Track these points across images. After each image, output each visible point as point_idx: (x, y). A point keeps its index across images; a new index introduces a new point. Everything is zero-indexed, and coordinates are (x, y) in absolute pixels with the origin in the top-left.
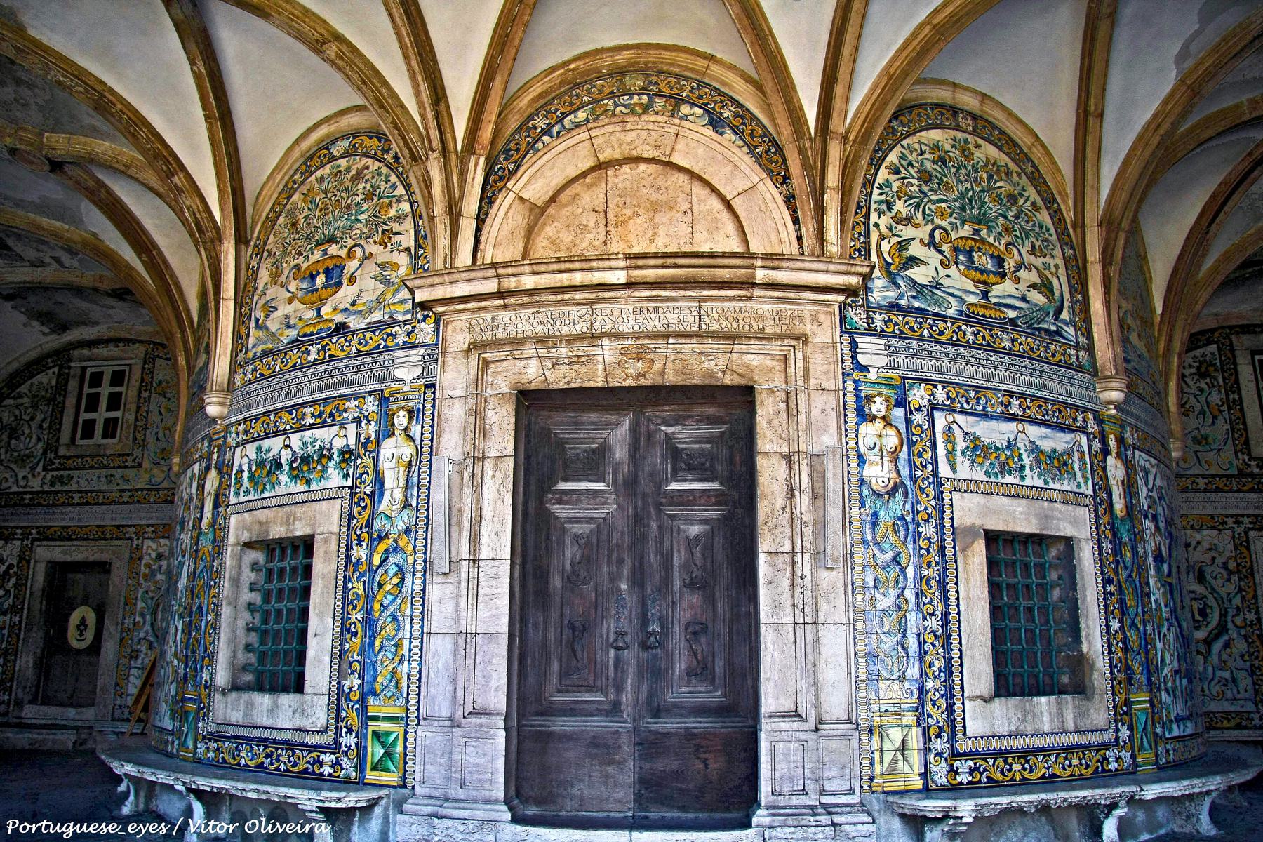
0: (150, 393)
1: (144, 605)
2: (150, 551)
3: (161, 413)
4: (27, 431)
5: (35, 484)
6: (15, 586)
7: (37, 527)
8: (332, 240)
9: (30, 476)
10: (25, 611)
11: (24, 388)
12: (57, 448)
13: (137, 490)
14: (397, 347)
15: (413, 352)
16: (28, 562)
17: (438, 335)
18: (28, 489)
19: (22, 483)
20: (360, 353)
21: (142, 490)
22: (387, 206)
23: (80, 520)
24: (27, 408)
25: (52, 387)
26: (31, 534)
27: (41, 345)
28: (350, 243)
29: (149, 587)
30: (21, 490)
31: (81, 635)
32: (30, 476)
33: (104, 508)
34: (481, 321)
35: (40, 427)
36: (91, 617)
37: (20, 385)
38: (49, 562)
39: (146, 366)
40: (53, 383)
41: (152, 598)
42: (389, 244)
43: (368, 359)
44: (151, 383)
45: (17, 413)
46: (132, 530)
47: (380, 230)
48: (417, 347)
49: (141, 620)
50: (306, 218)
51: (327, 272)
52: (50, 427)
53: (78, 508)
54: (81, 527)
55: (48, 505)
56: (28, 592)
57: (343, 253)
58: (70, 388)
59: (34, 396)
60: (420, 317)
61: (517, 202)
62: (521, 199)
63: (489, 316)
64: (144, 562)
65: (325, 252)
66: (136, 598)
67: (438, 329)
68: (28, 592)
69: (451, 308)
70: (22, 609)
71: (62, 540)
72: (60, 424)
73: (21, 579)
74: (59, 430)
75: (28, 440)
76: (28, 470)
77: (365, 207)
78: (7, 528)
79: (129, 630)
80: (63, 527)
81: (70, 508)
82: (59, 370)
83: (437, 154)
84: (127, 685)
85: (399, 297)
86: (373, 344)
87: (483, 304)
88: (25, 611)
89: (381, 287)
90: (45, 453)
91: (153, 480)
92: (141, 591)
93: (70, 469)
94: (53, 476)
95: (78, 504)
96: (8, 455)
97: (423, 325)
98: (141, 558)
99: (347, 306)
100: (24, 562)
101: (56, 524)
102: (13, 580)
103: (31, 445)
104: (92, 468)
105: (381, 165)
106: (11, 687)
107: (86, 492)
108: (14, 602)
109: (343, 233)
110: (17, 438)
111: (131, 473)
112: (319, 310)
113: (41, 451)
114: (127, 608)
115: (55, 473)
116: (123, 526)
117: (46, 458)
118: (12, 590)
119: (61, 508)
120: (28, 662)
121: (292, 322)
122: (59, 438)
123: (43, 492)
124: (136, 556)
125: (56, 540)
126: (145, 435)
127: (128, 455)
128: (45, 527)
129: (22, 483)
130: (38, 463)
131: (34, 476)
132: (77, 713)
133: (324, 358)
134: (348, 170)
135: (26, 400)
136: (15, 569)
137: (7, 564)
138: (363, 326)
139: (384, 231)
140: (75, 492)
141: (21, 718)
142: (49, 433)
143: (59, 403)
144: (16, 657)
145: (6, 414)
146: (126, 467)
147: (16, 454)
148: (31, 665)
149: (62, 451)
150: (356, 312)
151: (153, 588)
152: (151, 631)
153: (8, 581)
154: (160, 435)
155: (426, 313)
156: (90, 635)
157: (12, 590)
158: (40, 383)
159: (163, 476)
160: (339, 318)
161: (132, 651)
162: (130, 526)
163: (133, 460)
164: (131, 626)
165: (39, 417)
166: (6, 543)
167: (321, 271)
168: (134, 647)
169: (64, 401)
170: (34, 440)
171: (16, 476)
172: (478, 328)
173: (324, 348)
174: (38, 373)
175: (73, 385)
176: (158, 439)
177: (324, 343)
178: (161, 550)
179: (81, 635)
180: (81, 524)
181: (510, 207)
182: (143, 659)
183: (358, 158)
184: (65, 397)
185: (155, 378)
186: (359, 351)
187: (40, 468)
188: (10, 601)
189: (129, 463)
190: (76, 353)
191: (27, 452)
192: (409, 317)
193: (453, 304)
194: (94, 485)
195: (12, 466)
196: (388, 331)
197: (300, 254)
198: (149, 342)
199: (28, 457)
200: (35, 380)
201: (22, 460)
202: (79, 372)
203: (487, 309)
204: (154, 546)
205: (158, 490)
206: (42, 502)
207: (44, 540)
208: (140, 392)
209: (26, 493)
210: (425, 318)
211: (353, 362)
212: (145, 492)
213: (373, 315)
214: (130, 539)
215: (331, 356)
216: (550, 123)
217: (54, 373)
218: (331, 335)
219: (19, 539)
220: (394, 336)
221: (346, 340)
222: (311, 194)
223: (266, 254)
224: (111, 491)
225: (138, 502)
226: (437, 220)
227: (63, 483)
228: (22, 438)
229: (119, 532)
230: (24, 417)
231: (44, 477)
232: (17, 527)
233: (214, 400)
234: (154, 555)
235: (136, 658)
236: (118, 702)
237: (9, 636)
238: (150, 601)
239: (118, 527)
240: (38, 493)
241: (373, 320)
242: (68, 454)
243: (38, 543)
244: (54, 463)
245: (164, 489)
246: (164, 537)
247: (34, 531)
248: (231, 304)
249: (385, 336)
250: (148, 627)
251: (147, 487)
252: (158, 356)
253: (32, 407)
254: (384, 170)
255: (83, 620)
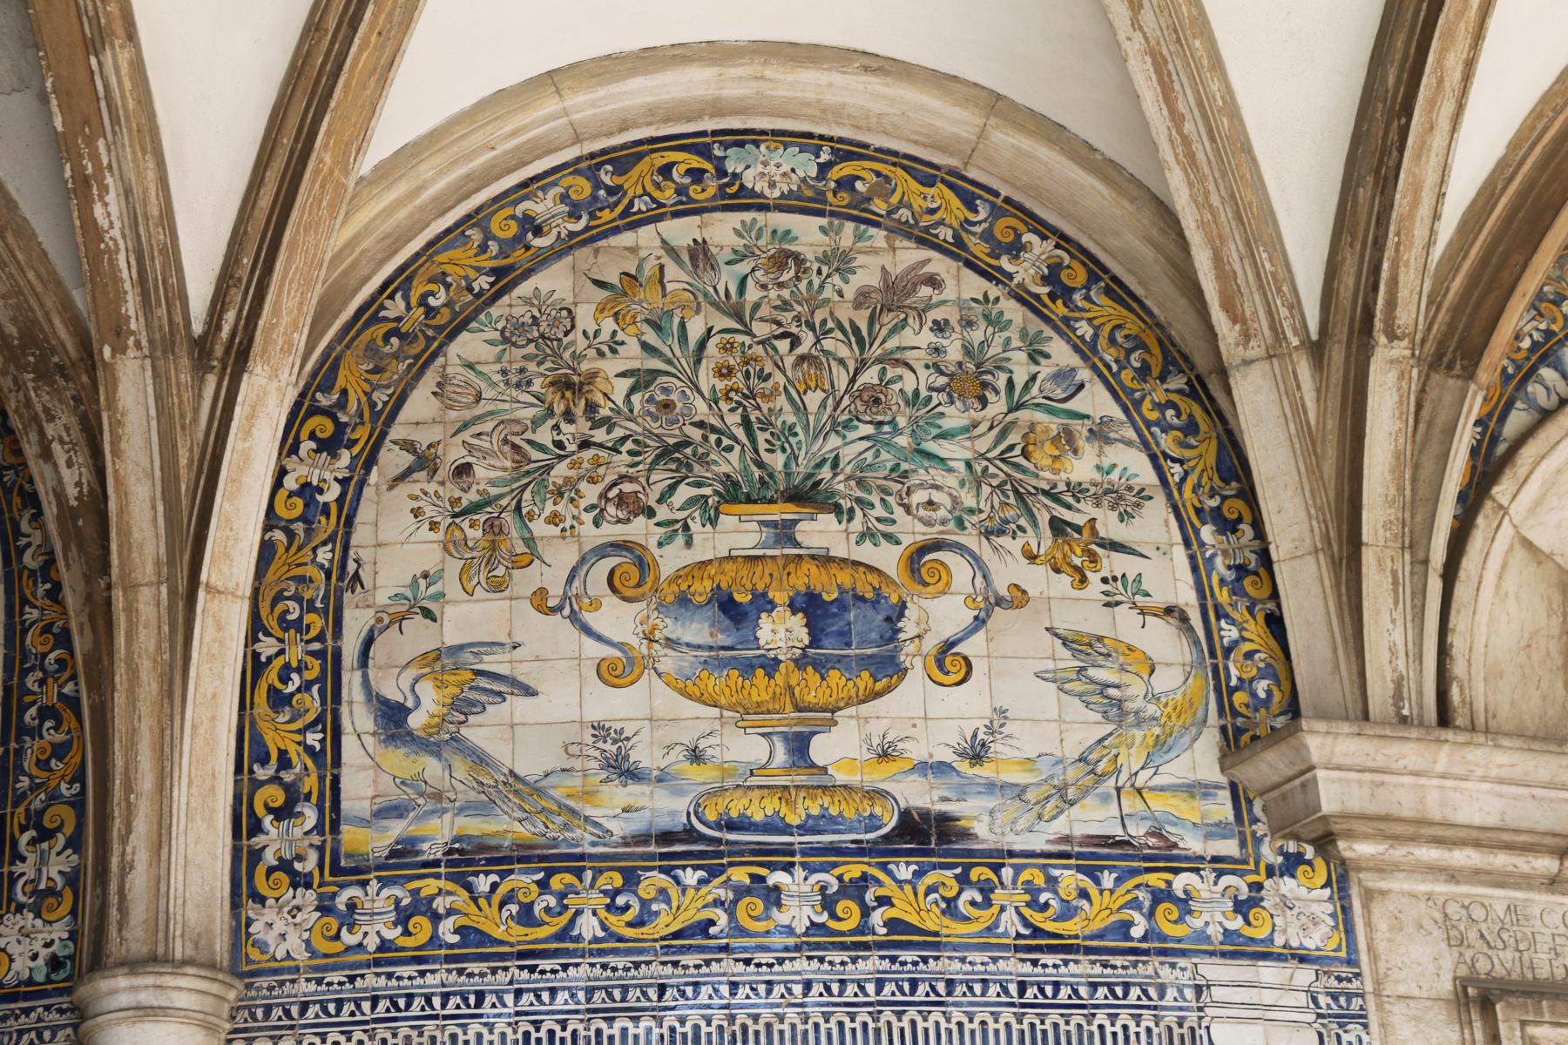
8: (808, 495)
14: (1200, 947)
15: (1268, 972)
17: (1349, 930)
20: (1035, 942)
22: (1055, 440)
28: (912, 531)
34: (1478, 913)
42: (1094, 579)
43: (1083, 968)
47: (1043, 518)
48: (1279, 957)
50: (642, 380)
51: (810, 606)
57: (888, 558)
60: (1269, 855)
61: (1520, 553)
62: (1527, 544)
63: (1500, 897)
65: (785, 533)
67: (1346, 910)
69: (1399, 853)
77: (954, 417)
83: (1401, 349)
85: (1176, 770)
86: (1093, 917)
87: (1501, 860)
89: (1086, 726)
97: (1288, 885)
99: (948, 756)
105: (994, 291)
109: (861, 483)
112: (799, 746)
121: (643, 755)
133: (863, 928)
134: (840, 262)
138: (1038, 843)
139: (1058, 526)
150: (991, 787)
155: (1292, 847)
160: (918, 795)
167: (780, 597)
172: (1472, 935)
173: (855, 889)
177: (853, 871)
181: (1504, 566)
183: (878, 236)
186: (1037, 932)
192: (1230, 848)
193: (1413, 839)
196: (1155, 880)
197: (635, 507)
203: (1501, 880)
210: (1292, 864)
211: (1013, 967)
213: (1075, 811)
215: (893, 925)
216: (1549, 334)
218: (884, 849)
220: (1184, 904)
221: (964, 880)
222: (650, 299)
223: (393, 459)
226: (1368, 557)
233: (182, 1000)
241: (1079, 831)
248: (237, 617)
249: (1144, 896)
254: (1012, 310)
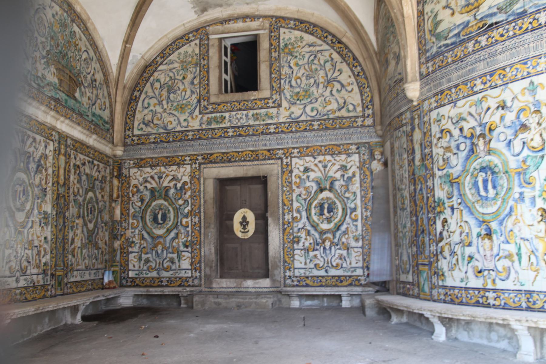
0: (279, 53)
1: (299, 205)
2: (298, 166)
3: (291, 67)
4: (182, 87)
5: (195, 124)
6: (191, 197)
7: (202, 155)
9: (190, 119)
10: (202, 214)
11: (173, 57)
12: (209, 98)
13: (280, 123)
16: (199, 179)
18: (189, 128)
19: (185, 124)
21: (285, 123)
23: (236, 147)
24: (178, 71)
25: (196, 55)
26: (197, 159)
27: (184, 25)
29: (301, 192)
30: (184, 129)
31: (244, 228)
32: (190, 119)
33: (254, 138)
35: (192, 83)
36: (251, 217)
37: (170, 55)
38: (215, 179)
39: (272, 34)
40: (197, 51)
41: (305, 200)
44: (279, 46)
45: (171, 74)
46: (281, 152)
49: (298, 215)
52: (200, 83)
53: (233, 139)
54: (238, 152)
55: (207, 139)
56: (202, 201)
58: (211, 54)
59: (182, 62)
64: (294, 174)
66: (292, 200)
68: (202, 201)
70: (200, 212)
71: (223, 163)
72: (208, 80)
73: (195, 192)
74: (208, 85)
75: (183, 93)
76: (187, 114)
78: (178, 157)
79: (289, 223)
80: (223, 153)
81: (226, 139)
82: (200, 42)
84: (293, 261)
88: (202, 214)
90: (199, 101)
91: (293, 116)
92: (294, 196)
93: (222, 112)
94: (208, 118)
95: (232, 136)
96: (170, 104)
98: (291, 172)
100: (195, 180)
101: (216, 151)
102: (189, 193)
103: (186, 97)
104: (240, 110)
106: (200, 267)
107: (238, 127)
108: (192, 209)
110: (174, 93)
111: (274, 111)
113: (196, 100)
114: (286, 207)
115: (210, 116)
116: (273, 150)
117: (200, 105)
118: (189, 200)
119: (219, 140)
120: (210, 249)
122: (209, 90)
123: (202, 130)
124: (287, 170)
125: (218, 163)
126: (280, 83)
127: (268, 99)
128: (208, 154)
129: (185, 124)
130: (195, 109)
131: (192, 118)
132: (255, 283)
135: (176, 65)
136: (189, 185)
137: (182, 182)
140: (228, 128)
141: (212, 288)
142: (200, 87)
143: (204, 65)
144: (200, 245)
145: (163, 76)
146: (268, 107)
147: (175, 104)
148: (213, 250)
149: (213, 99)
151: (304, 192)
152: (307, 224)
153: (185, 194)
154: (293, 83)
156: (251, 228)
157: (189, 200)
158: (186, 52)
159: (301, 112)
161: (294, 238)
162: (279, 149)
163: (274, 102)
164: (290, 220)
165: (190, 77)
166: (179, 167)
168: (295, 235)
169: (208, 64)
170: (188, 93)
171: (178, 119)
174: (183, 45)
175: (213, 53)
176: (291, 86)
178: (306, 165)
179: (244, 228)
180: (237, 150)
182: (304, 243)
184: (208, 60)
185: (281, 41)
187: (197, 112)
188: (189, 208)
189: (271, 105)
190: (211, 29)
191: (184, 102)
194: (243, 121)
195: (176, 113)
198: (272, 17)
199: (186, 106)
200: (182, 50)
201: (181, 108)
202: (217, 43)
204: (301, 162)
205: (298, 122)
206: (202, 136)
207: (208, 163)
208: (270, 52)
209: (188, 131)
212: (287, 125)
214: (280, 158)
217: (196, 44)
219: (188, 164)
224: (259, 125)
225: (282, 132)
227: (217, 122)
228: (179, 92)
229: (271, 154)
230: (177, 77)
231: (202, 118)
232: (186, 156)
234: (302, 169)
235: (298, 242)
236: (288, 274)
237: (192, 232)
238: (303, 202)
239: (269, 150)
240: (198, 130)
242: (219, 101)
243: (205, 166)
244: (207, 109)
245: (303, 121)
246: (308, 155)
247: (200, 158)
250: (304, 219)
251: (288, 120)
252: (281, 26)
253: (183, 69)
255: (244, 218)
